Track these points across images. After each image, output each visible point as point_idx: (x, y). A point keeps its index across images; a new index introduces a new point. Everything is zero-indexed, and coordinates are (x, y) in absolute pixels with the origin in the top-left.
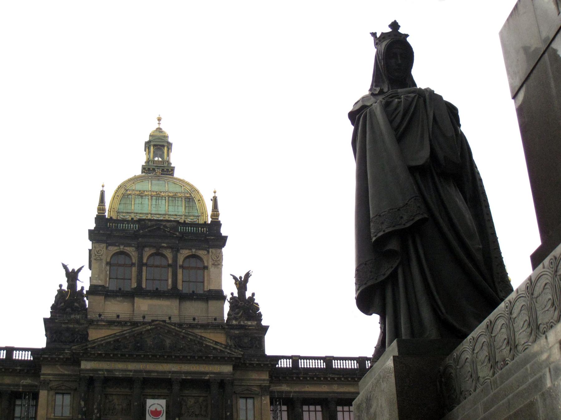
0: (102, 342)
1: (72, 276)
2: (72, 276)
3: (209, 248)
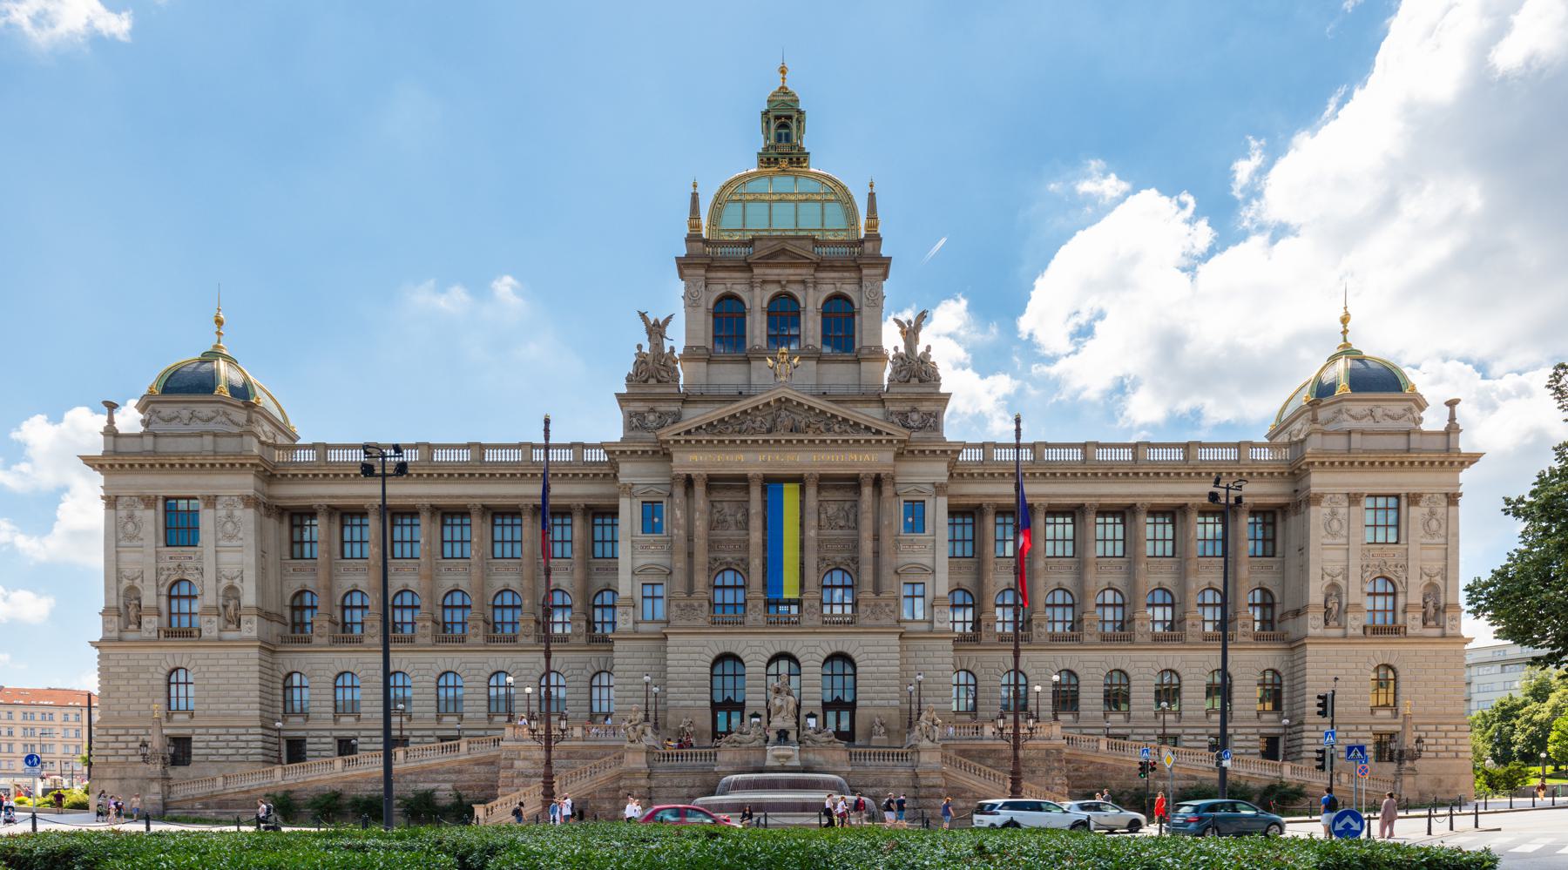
1: (656, 330)
2: (656, 330)
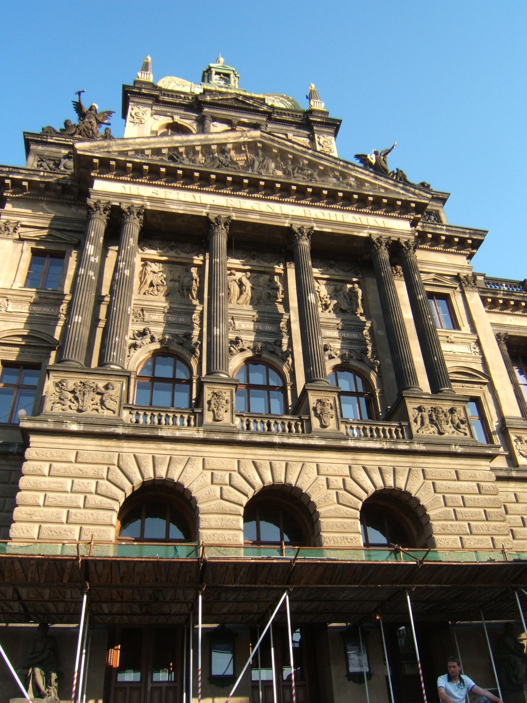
0: (144, 147)
3: (313, 135)
